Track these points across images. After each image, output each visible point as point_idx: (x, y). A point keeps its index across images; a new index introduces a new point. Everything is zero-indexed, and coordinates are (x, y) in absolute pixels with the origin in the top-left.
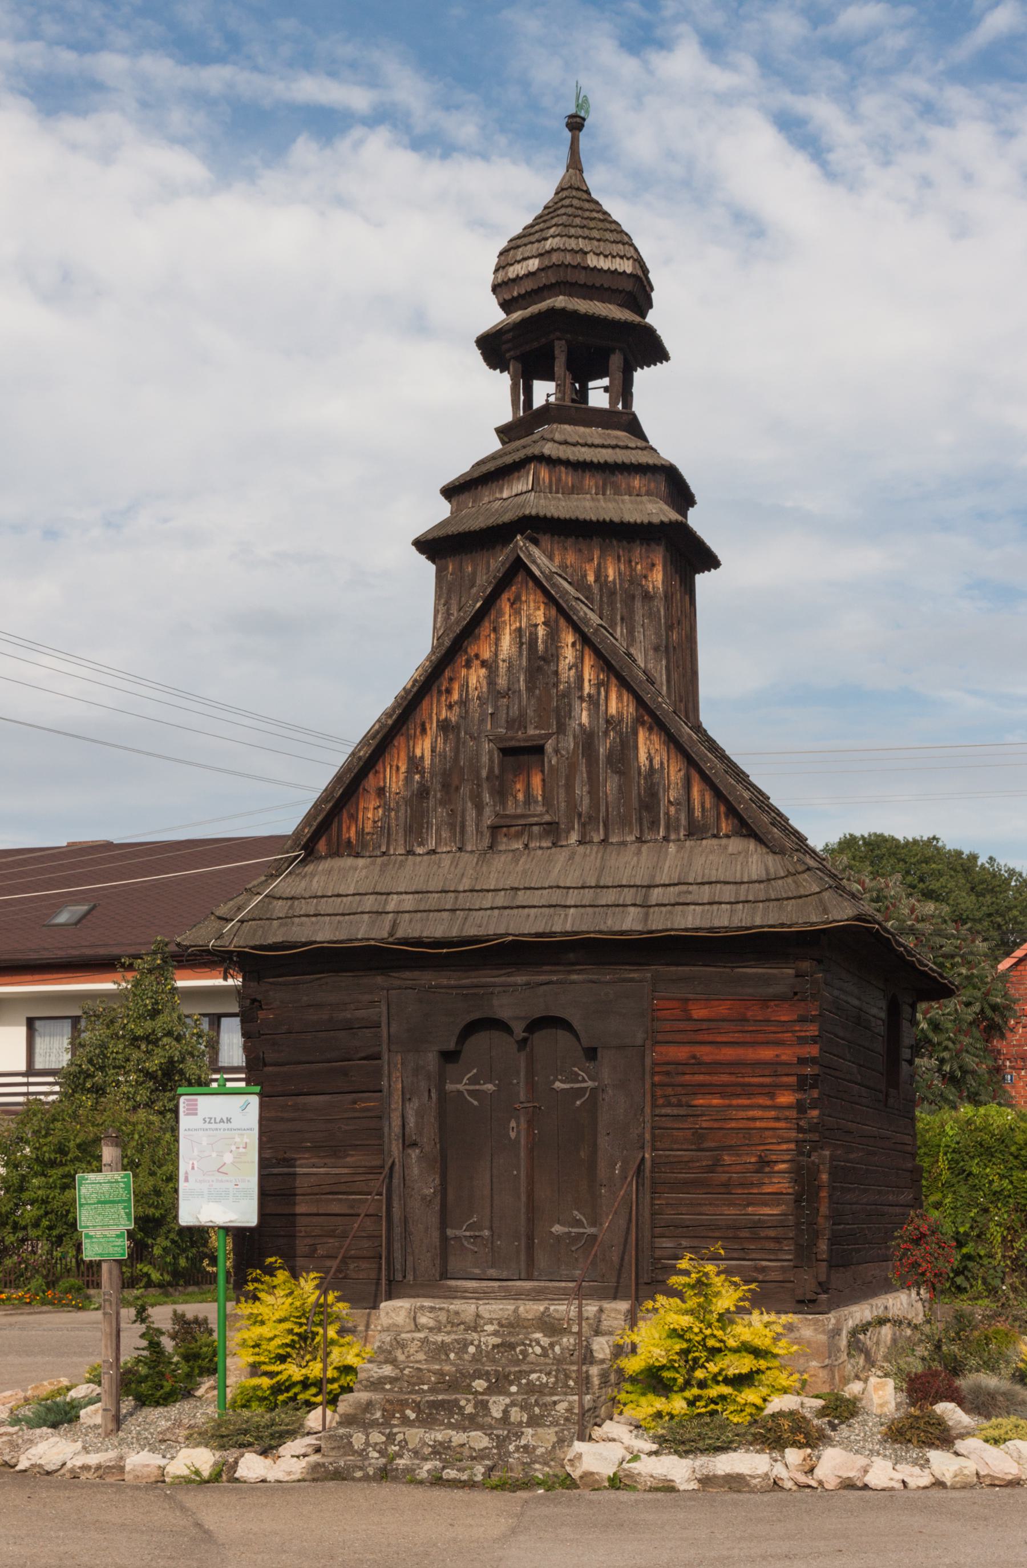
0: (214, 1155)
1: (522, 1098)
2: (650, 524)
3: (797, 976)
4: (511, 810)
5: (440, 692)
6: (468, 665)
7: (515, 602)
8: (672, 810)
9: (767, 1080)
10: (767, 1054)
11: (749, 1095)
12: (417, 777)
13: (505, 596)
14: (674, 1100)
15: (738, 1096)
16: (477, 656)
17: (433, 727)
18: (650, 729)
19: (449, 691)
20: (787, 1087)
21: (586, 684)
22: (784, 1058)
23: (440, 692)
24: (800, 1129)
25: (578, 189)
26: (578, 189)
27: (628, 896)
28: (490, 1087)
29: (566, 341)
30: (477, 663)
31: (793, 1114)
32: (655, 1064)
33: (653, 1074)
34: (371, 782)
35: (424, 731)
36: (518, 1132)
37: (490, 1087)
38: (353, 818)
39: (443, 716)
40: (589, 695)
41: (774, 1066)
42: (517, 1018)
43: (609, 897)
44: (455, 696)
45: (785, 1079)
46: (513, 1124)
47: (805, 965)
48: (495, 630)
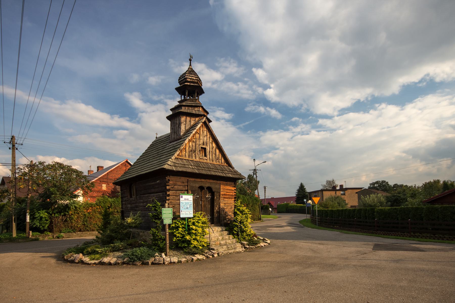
0: (186, 206)
1: (203, 198)
9: (231, 197)
10: (231, 194)
18: (218, 149)
22: (233, 194)
28: (198, 196)
31: (234, 201)
36: (202, 203)
37: (198, 196)
45: (233, 197)
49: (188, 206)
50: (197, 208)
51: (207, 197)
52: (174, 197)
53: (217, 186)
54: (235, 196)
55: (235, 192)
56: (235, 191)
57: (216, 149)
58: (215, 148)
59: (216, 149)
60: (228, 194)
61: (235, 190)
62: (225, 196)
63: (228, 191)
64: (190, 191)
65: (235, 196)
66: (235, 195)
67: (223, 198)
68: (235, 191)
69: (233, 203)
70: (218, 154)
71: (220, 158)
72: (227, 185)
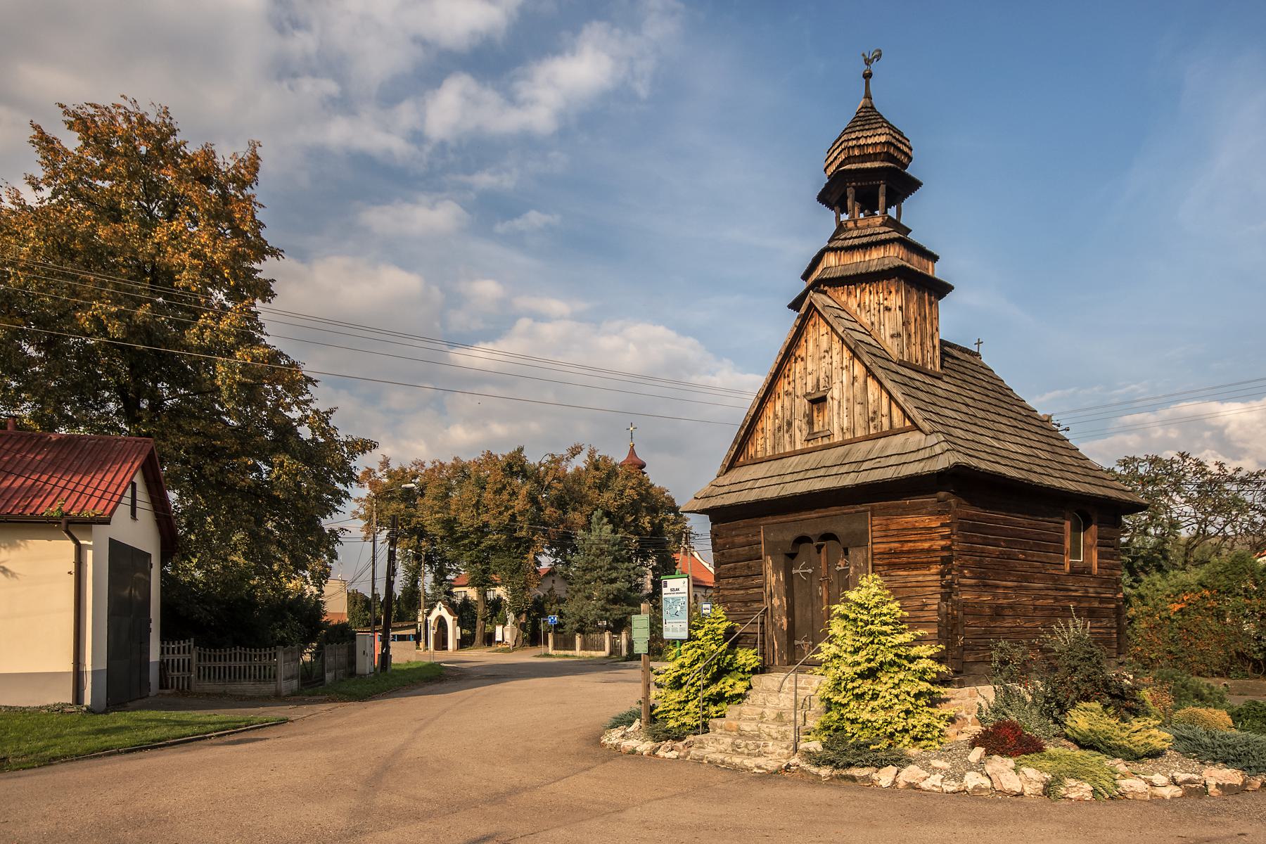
2: (883, 270)
3: (939, 502)
4: (816, 430)
5: (785, 377)
6: (795, 362)
7: (814, 326)
8: (884, 419)
9: (925, 560)
10: (926, 545)
11: (917, 569)
12: (777, 421)
13: (810, 323)
14: (883, 572)
15: (913, 569)
16: (799, 356)
17: (782, 395)
19: (788, 376)
20: (936, 562)
21: (845, 360)
22: (934, 547)
23: (785, 377)
24: (942, 587)
25: (866, 107)
26: (866, 107)
27: (853, 467)
28: (810, 571)
29: (853, 187)
30: (799, 359)
31: (939, 577)
32: (873, 554)
33: (873, 559)
34: (759, 426)
35: (779, 397)
37: (810, 571)
38: (753, 444)
39: (786, 390)
40: (846, 366)
41: (929, 550)
42: (815, 535)
43: (845, 469)
44: (791, 379)
46: (820, 588)
47: (942, 494)
48: (806, 341)
49: (679, 609)
50: (810, 608)
51: (838, 568)
52: (731, 580)
53: (856, 526)
54: (945, 554)
55: (943, 537)
56: (947, 531)
57: (866, 382)
58: (861, 380)
59: (866, 382)
60: (907, 547)
61: (943, 525)
62: (897, 560)
63: (907, 538)
64: (769, 557)
65: (945, 554)
66: (944, 548)
67: (886, 568)
68: (947, 531)
69: (935, 583)
70: (876, 397)
71: (885, 410)
72: (906, 511)
